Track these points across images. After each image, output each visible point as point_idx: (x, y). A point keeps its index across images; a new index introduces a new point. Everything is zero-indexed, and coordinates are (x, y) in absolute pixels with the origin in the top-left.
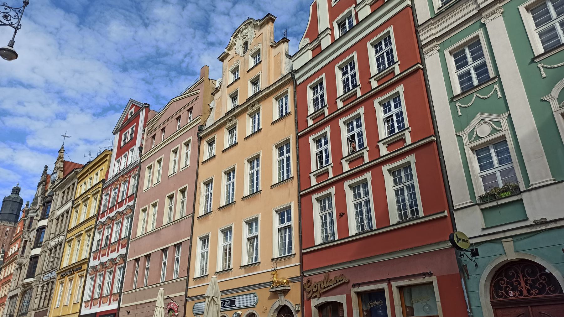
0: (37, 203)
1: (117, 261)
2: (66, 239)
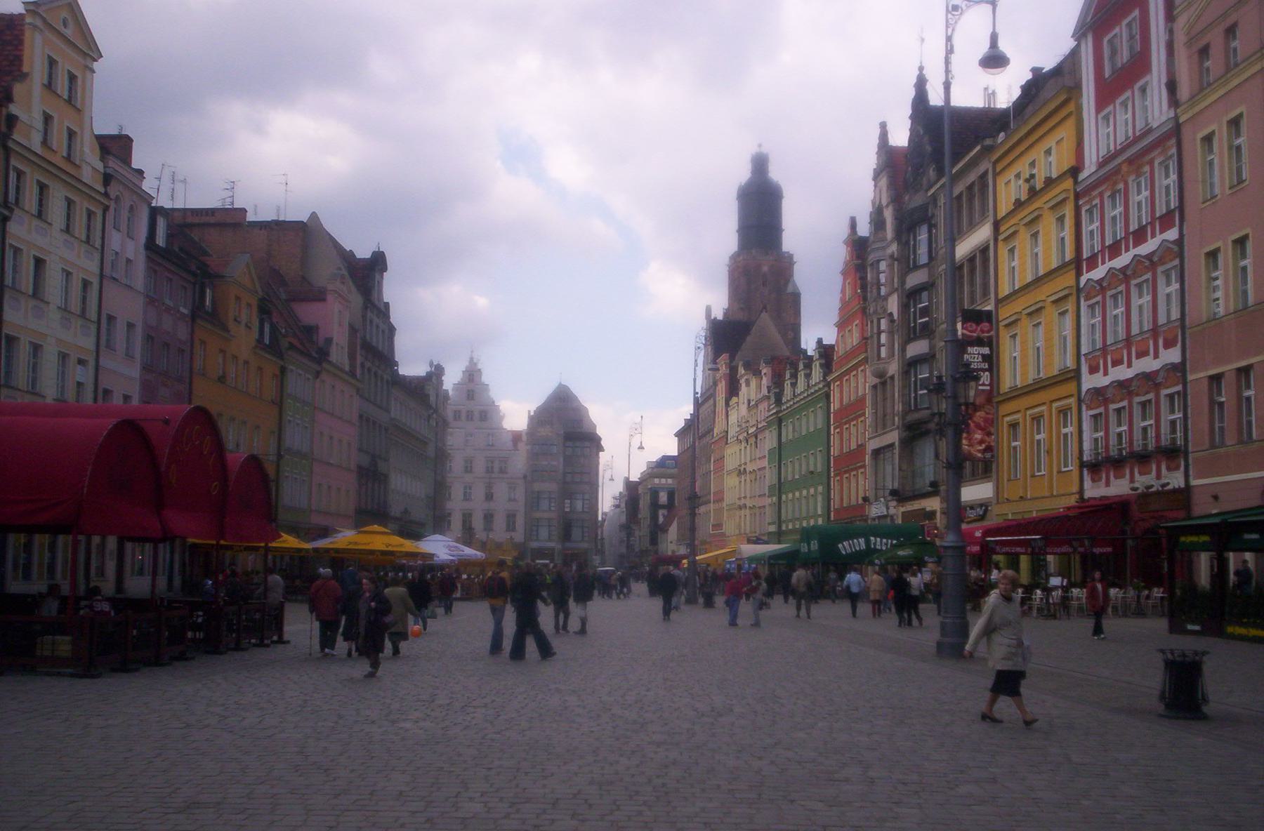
1: (1159, 380)
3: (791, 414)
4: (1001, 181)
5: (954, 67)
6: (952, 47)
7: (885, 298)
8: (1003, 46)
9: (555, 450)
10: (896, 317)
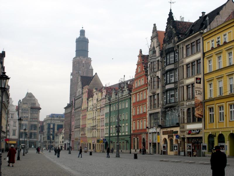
4: (206, 42)
10: (160, 77)
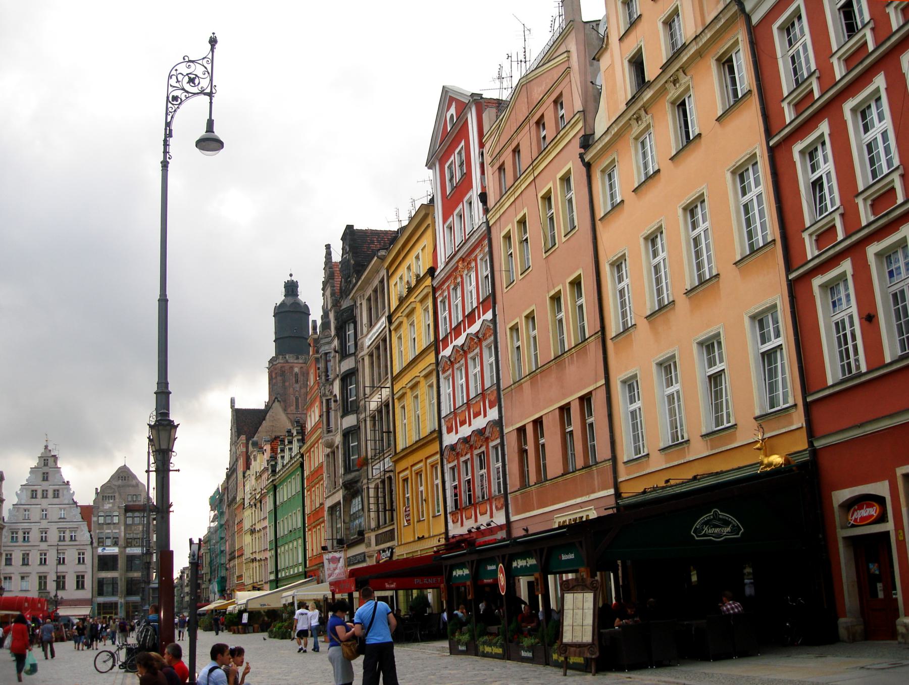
0: (329, 323)
1: (487, 434)
2: (393, 394)
3: (281, 483)
4: (392, 283)
5: (172, 149)
6: (171, 131)
7: (332, 384)
8: (218, 132)
9: (116, 520)
